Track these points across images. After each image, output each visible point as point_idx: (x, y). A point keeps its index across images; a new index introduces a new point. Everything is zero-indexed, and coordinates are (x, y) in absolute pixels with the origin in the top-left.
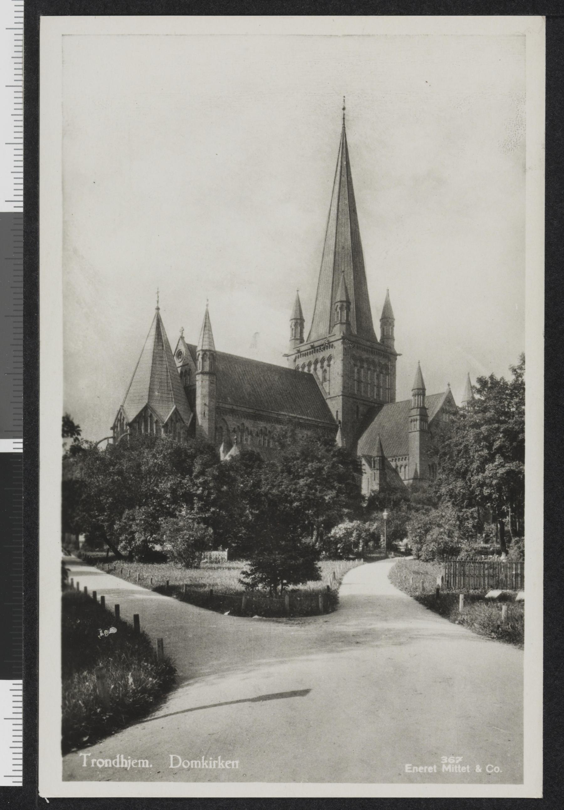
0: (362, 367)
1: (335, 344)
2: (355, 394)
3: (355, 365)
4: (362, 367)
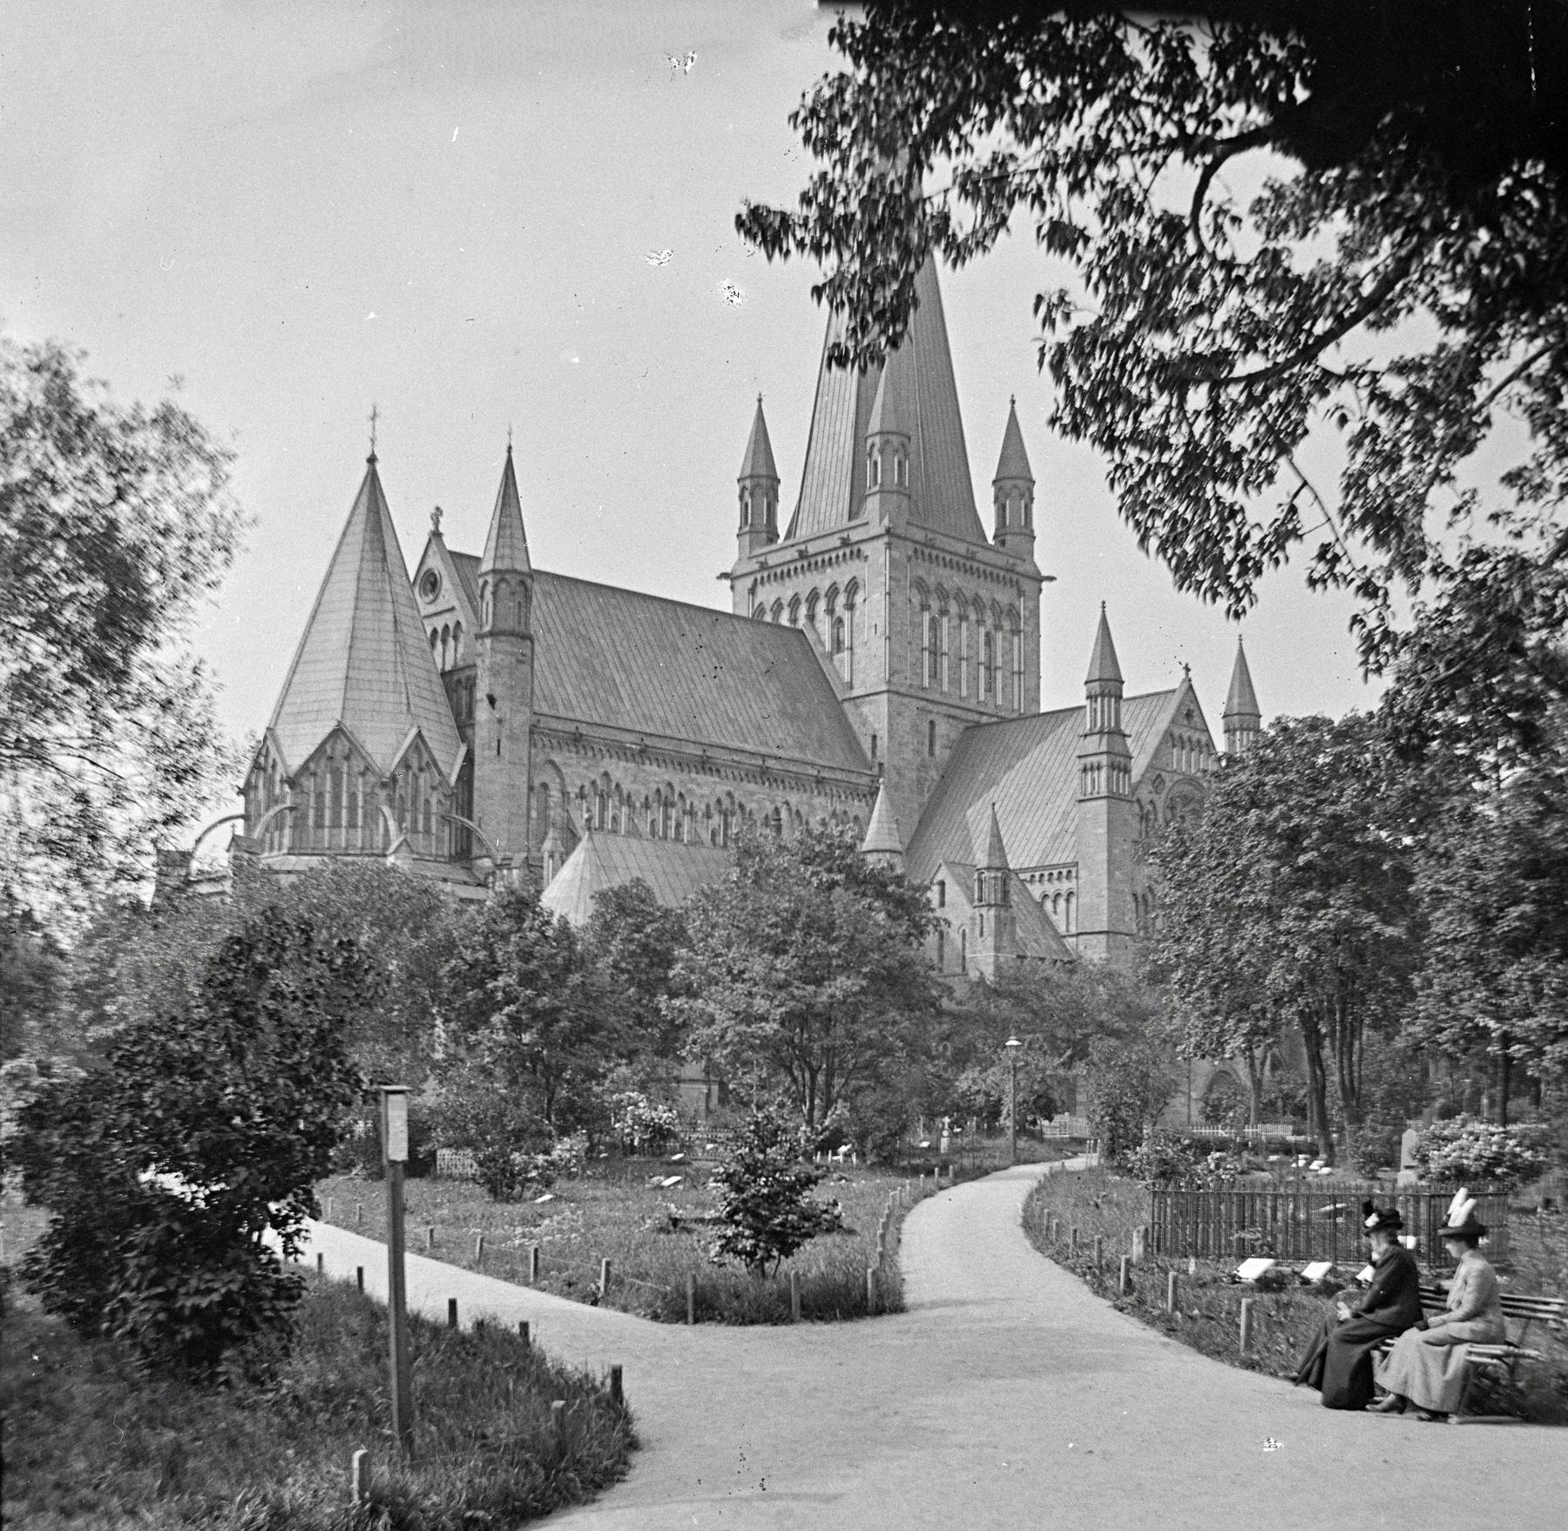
0: (944, 612)
1: (866, 549)
2: (923, 689)
3: (925, 607)
4: (944, 612)
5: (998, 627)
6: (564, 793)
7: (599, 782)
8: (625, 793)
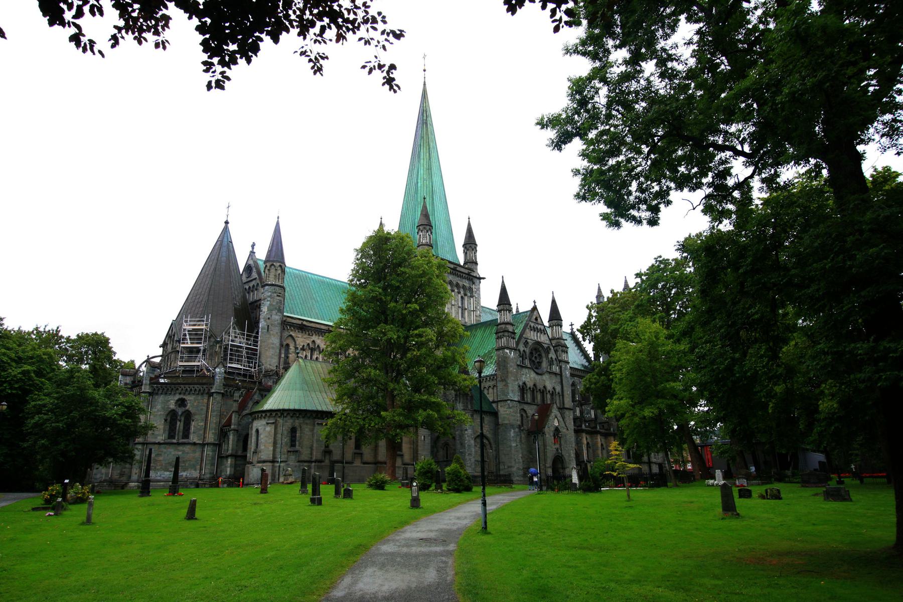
5: (465, 295)
6: (296, 348)
7: (311, 344)
8: (321, 349)
